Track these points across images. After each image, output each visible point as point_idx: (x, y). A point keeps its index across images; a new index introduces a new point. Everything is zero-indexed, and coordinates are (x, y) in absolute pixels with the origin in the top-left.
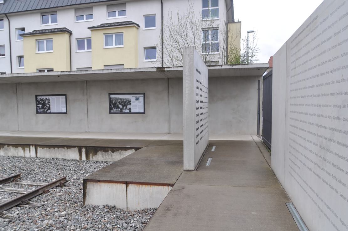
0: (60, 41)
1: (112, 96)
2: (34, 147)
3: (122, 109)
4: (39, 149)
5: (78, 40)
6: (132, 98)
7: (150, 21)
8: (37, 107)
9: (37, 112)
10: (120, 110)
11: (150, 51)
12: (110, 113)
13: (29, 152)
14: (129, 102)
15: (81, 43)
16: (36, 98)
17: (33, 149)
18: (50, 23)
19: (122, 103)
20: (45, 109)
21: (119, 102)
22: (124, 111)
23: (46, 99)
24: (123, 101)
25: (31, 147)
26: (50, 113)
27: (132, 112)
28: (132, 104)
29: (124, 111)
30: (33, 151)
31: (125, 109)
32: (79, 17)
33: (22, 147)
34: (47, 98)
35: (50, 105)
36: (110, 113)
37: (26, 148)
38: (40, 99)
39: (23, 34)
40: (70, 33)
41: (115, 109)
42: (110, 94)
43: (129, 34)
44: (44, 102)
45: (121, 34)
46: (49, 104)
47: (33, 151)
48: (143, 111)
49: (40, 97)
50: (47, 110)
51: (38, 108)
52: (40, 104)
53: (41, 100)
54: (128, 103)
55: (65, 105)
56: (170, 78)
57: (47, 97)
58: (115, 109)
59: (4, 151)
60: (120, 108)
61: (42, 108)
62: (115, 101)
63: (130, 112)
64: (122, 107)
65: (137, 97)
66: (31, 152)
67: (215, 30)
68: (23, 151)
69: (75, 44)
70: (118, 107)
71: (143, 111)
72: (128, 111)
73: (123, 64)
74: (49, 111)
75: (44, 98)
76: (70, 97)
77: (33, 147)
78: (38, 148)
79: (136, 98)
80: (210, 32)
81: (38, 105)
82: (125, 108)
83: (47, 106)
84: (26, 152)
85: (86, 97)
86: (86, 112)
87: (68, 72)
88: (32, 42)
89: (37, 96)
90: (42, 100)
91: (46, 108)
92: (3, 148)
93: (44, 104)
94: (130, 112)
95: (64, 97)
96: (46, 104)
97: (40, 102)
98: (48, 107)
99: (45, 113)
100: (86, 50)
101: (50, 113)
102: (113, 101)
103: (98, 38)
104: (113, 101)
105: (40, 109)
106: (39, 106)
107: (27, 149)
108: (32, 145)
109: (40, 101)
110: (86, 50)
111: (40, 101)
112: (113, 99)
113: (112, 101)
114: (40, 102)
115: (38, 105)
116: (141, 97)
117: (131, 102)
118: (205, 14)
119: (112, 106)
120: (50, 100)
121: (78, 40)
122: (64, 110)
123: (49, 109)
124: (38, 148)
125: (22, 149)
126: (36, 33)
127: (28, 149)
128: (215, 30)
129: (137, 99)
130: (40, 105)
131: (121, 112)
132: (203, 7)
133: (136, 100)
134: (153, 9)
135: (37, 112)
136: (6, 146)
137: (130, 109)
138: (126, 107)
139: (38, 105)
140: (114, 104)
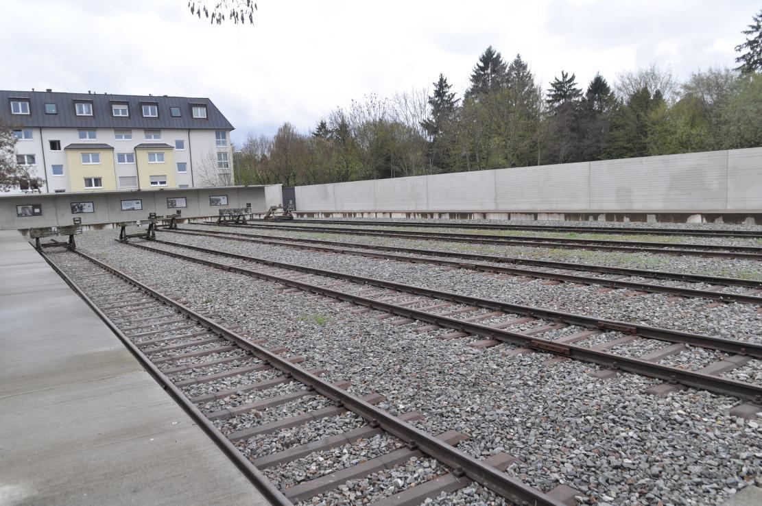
0: (103, 155)
5: (134, 156)
6: (221, 198)
7: (180, 145)
11: (181, 167)
14: (220, 200)
15: (121, 158)
17: (210, 218)
18: (88, 139)
32: (117, 137)
39: (55, 145)
40: (112, 149)
43: (167, 154)
45: (162, 154)
61: (171, 205)
67: (225, 154)
69: (116, 157)
73: (165, 176)
76: (188, 198)
88: (76, 156)
93: (172, 203)
103: (143, 156)
116: (225, 197)
118: (218, 143)
121: (134, 156)
126: (72, 147)
128: (225, 154)
132: (217, 138)
134: (182, 136)
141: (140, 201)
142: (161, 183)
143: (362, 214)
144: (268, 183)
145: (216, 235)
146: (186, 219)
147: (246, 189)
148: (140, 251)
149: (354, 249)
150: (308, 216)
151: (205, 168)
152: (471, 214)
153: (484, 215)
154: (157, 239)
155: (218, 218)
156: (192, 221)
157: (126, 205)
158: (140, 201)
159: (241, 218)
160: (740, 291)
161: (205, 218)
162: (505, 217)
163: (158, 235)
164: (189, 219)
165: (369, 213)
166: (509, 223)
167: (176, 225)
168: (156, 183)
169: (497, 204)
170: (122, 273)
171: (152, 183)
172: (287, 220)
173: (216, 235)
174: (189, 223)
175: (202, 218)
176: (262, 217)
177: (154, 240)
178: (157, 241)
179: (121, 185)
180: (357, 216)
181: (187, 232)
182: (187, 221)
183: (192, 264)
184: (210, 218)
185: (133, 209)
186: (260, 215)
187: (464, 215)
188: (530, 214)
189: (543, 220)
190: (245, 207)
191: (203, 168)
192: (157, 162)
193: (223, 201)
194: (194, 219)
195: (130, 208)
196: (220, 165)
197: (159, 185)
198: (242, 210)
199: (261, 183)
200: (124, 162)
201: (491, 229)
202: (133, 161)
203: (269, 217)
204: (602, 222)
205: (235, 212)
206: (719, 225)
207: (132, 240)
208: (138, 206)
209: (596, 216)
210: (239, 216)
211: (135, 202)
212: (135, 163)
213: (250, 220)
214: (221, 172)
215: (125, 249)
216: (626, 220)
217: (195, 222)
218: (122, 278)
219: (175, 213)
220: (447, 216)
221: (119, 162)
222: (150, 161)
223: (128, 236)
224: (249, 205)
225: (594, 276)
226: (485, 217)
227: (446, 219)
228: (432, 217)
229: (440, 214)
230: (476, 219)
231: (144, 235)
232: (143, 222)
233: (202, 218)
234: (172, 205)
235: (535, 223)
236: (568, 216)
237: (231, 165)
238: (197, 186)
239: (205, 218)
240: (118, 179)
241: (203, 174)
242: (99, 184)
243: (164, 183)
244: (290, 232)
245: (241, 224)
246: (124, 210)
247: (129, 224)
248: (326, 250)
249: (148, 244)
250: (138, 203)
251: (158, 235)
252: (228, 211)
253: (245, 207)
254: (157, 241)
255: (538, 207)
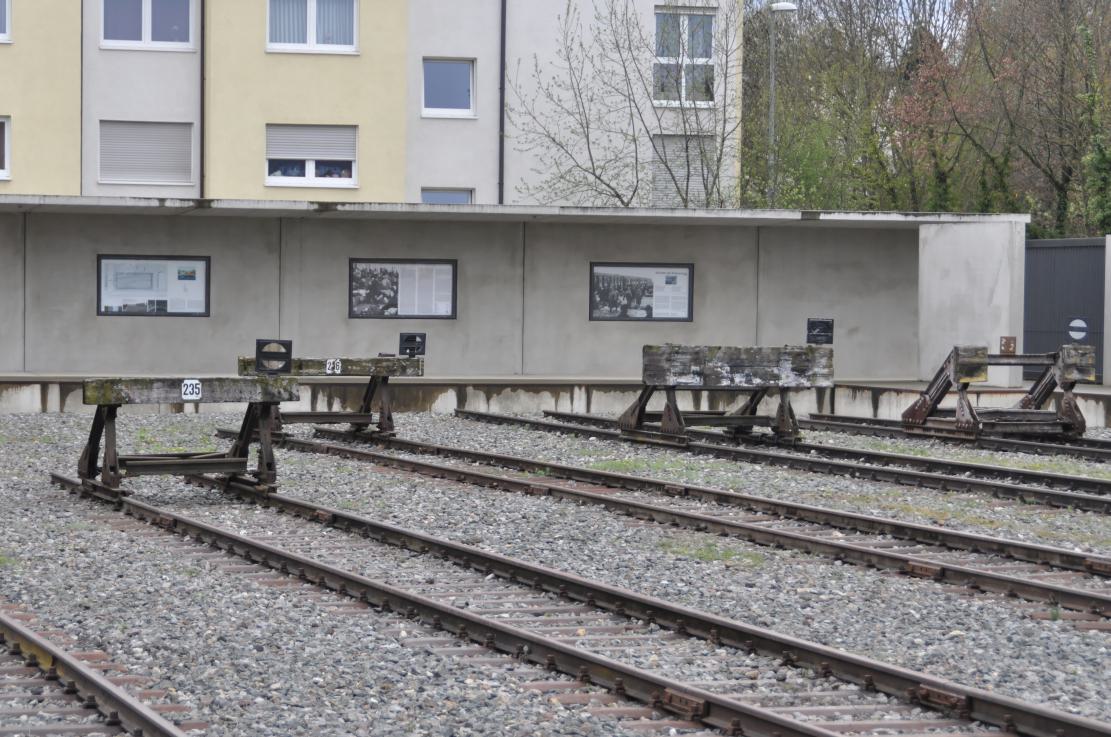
1: (598, 270)
2: (583, 389)
3: (625, 308)
4: (596, 395)
6: (656, 276)
8: (351, 295)
9: (352, 315)
10: (619, 309)
12: (591, 318)
13: (569, 402)
14: (648, 289)
16: (351, 269)
17: (580, 395)
19: (625, 290)
20: (377, 303)
21: (619, 288)
22: (632, 313)
23: (384, 272)
24: (631, 285)
25: (576, 390)
26: (396, 317)
27: (654, 316)
28: (655, 294)
29: (632, 313)
30: (580, 399)
31: (636, 308)
33: (551, 392)
34: (386, 271)
35: (396, 292)
36: (591, 318)
37: (562, 394)
38: (363, 271)
41: (607, 308)
42: (592, 265)
44: (374, 283)
46: (392, 289)
47: (580, 399)
48: (684, 314)
49: (361, 266)
50: (387, 307)
51: (354, 301)
52: (362, 286)
53: (365, 274)
54: (643, 291)
55: (449, 294)
56: (763, 227)
57: (389, 267)
58: (607, 308)
59: (501, 403)
60: (619, 304)
61: (368, 299)
62: (606, 285)
63: (649, 318)
64: (625, 302)
65: (671, 275)
66: (575, 401)
68: (553, 401)
70: (614, 303)
71: (684, 314)
72: (642, 314)
73: (355, 127)
74: (392, 311)
75: (376, 267)
76: (469, 269)
77: (580, 389)
78: (594, 392)
79: (667, 278)
80: (684, 22)
81: (355, 292)
82: (634, 304)
83: (385, 295)
84: (561, 402)
85: (519, 271)
86: (519, 315)
87: (579, 210)
89: (352, 261)
90: (371, 274)
91: (381, 301)
92: (499, 394)
93: (375, 289)
94: (649, 318)
95: (448, 268)
96: (385, 288)
97: (364, 280)
98: (389, 297)
99: (381, 316)
100: (147, 42)
101: (396, 317)
102: (601, 285)
104: (601, 285)
105: (360, 303)
106: (360, 295)
107: (565, 397)
108: (580, 386)
109: (363, 277)
110: (147, 42)
111: (363, 277)
112: (601, 278)
113: (598, 282)
114: (364, 280)
115: (356, 289)
116: (682, 276)
117: (652, 287)
119: (598, 299)
120: (397, 277)
122: (444, 308)
123: (393, 303)
124: (594, 392)
125: (553, 396)
127: (568, 395)
128: (703, 20)
129: (671, 281)
130: (363, 292)
131: (624, 317)
133: (667, 283)
135: (352, 315)
136: (509, 389)
137: (649, 309)
138: (639, 302)
139: (355, 292)
140: (605, 295)
141: (199, 267)
142: (327, 168)
144: (940, 206)
145: (617, 495)
146: (442, 387)
147: (808, 235)
148: (189, 553)
151: (578, 94)
154: (281, 493)
155: (632, 399)
156: (478, 404)
157: (122, 284)
158: (199, 267)
159: (769, 407)
161: (557, 388)
163: (295, 475)
164: (461, 389)
167: (387, 423)
168: (294, 167)
170: (94, 675)
171: (277, 166)
172: (1052, 438)
173: (617, 495)
174: (461, 413)
175: (534, 388)
176: (894, 409)
177: (268, 500)
178: (285, 506)
179: (107, 167)
181: (450, 464)
182: (447, 402)
183: (485, 661)
184: (580, 395)
185: (160, 309)
186: (876, 394)
190: (798, 339)
191: (567, 96)
192: (312, 45)
193: (668, 296)
194: (491, 389)
195: (140, 298)
196: (666, 82)
197: (310, 178)
198: (779, 355)
199: (891, 201)
200: (138, 36)
202: (186, 39)
203: (934, 411)
205: (736, 366)
207: (143, 487)
208: (186, 296)
210: (757, 395)
211: (174, 267)
212: (192, 44)
213: (817, 422)
214: (670, 124)
215: (108, 533)
217: (495, 408)
218: (91, 706)
219: (392, 348)
221: (109, 34)
222: (273, 39)
223: (123, 462)
224: (822, 330)
231: (215, 462)
232: (213, 388)
233: (534, 388)
234: (374, 302)
237: (730, 87)
238: (522, 201)
239: (557, 388)
240: (93, 131)
241: (564, 127)
242: (324, 170)
243: (342, 168)
244: (1064, 518)
245: (762, 440)
246: (109, 313)
247: (135, 394)
249: (233, 520)
250: (191, 276)
251: (295, 475)
252: (698, 356)
253: (798, 339)
254: (285, 506)
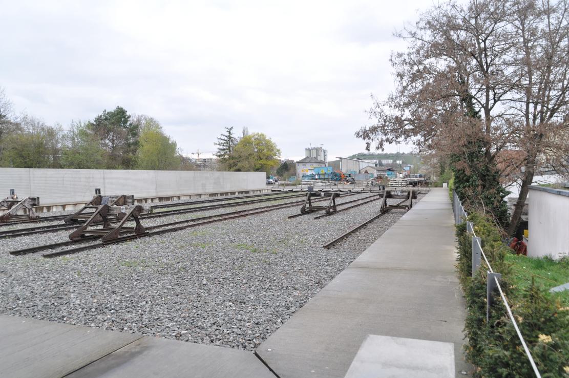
143: (64, 206)
149: (285, 206)
150: (138, 202)
152: (172, 197)
153: (179, 197)
160: (216, 219)
162: (188, 198)
165: (75, 204)
166: (190, 201)
169: (157, 192)
180: (54, 209)
181: (205, 221)
187: (168, 198)
188: (198, 195)
189: (204, 198)
201: (188, 205)
204: (219, 197)
206: (244, 195)
209: (217, 194)
216: (219, 195)
220: (157, 200)
225: (273, 208)
226: (179, 198)
227: (207, 198)
228: (146, 202)
229: (152, 199)
230: (175, 201)
235: (200, 200)
236: (211, 195)
248: (175, 230)
255: (200, 192)
